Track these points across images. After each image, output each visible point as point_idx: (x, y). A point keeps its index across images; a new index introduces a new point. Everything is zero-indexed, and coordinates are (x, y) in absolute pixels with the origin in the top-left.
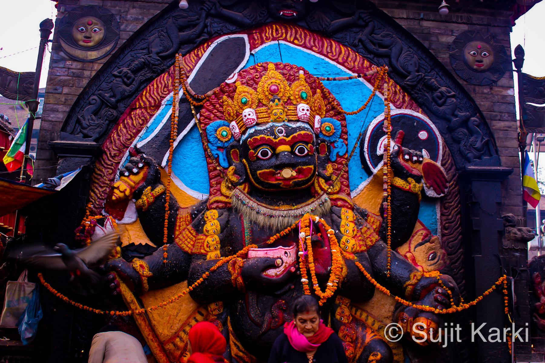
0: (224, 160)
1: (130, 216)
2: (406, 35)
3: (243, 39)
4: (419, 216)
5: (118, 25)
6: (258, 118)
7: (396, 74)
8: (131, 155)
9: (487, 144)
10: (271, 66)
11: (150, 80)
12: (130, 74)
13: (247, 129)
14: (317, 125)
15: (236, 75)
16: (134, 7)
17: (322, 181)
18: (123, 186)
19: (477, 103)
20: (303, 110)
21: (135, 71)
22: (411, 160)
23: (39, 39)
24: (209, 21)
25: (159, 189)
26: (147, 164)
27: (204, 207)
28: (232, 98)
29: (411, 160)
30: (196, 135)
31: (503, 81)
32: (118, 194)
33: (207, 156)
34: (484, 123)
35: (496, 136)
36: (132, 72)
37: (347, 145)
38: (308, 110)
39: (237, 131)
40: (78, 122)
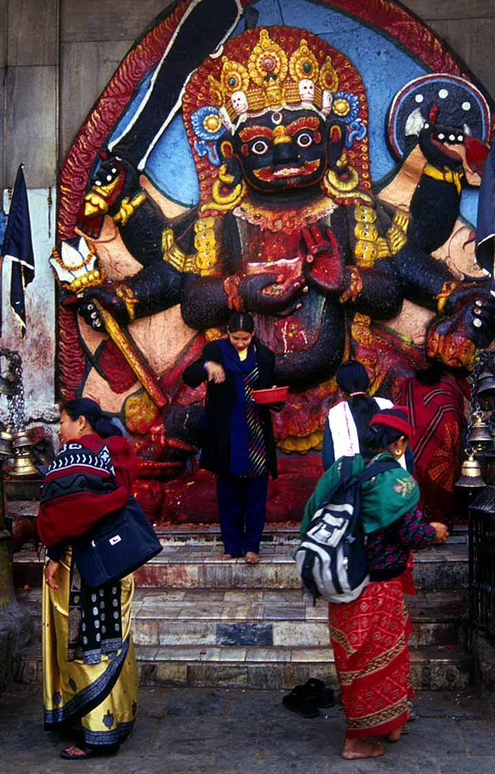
0: (214, 156)
4: (461, 211)
6: (249, 104)
13: (238, 117)
14: (326, 103)
15: (222, 48)
17: (332, 177)
20: (305, 88)
25: (138, 201)
27: (193, 215)
28: (219, 79)
29: (446, 139)
30: (179, 126)
32: (89, 210)
33: (194, 154)
37: (367, 126)
38: (311, 87)
39: (227, 118)
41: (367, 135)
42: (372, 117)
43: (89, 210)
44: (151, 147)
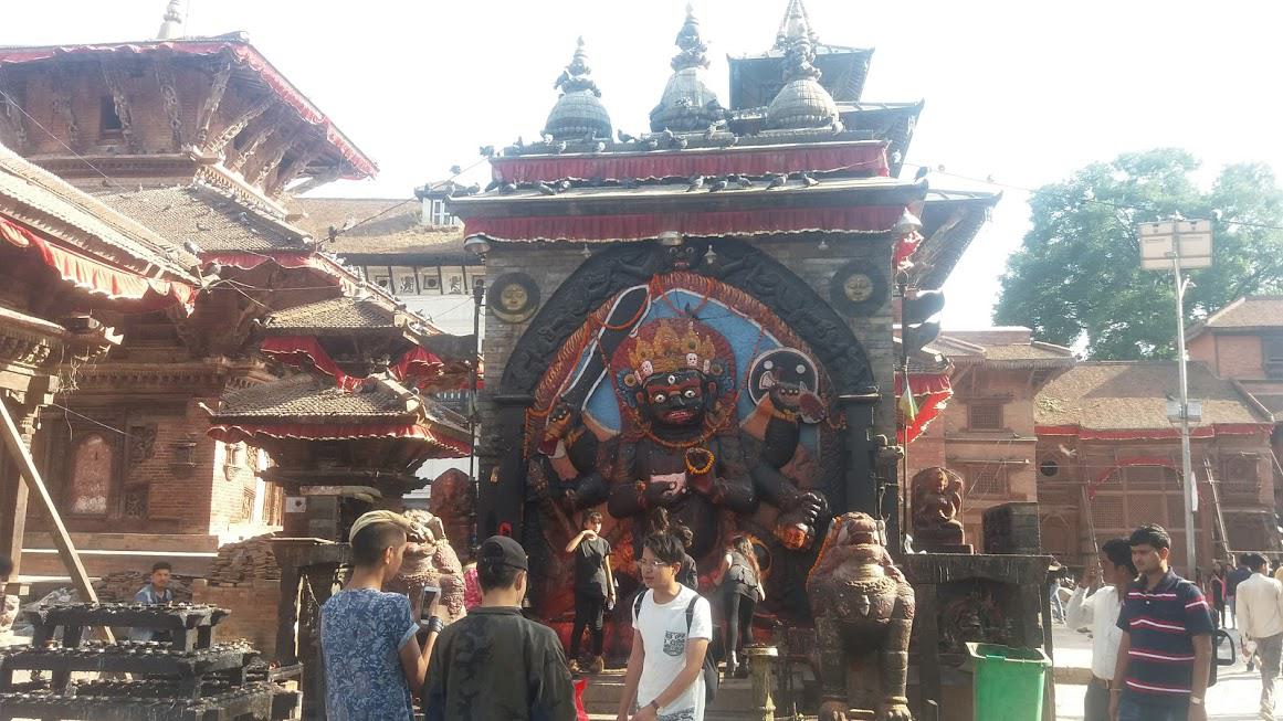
1: (560, 452)
2: (789, 273)
3: (645, 289)
5: (538, 290)
7: (782, 311)
8: (557, 403)
9: (864, 370)
10: (664, 322)
11: (570, 335)
12: (552, 332)
14: (706, 369)
16: (550, 272)
18: (552, 431)
19: (856, 334)
21: (555, 329)
22: (787, 392)
23: (474, 305)
24: (614, 276)
26: (570, 410)
31: (882, 310)
34: (862, 353)
35: (873, 363)
36: (554, 330)
37: (735, 382)
40: (513, 375)
41: (735, 387)
42: (739, 374)
43: (548, 437)
44: (590, 395)
